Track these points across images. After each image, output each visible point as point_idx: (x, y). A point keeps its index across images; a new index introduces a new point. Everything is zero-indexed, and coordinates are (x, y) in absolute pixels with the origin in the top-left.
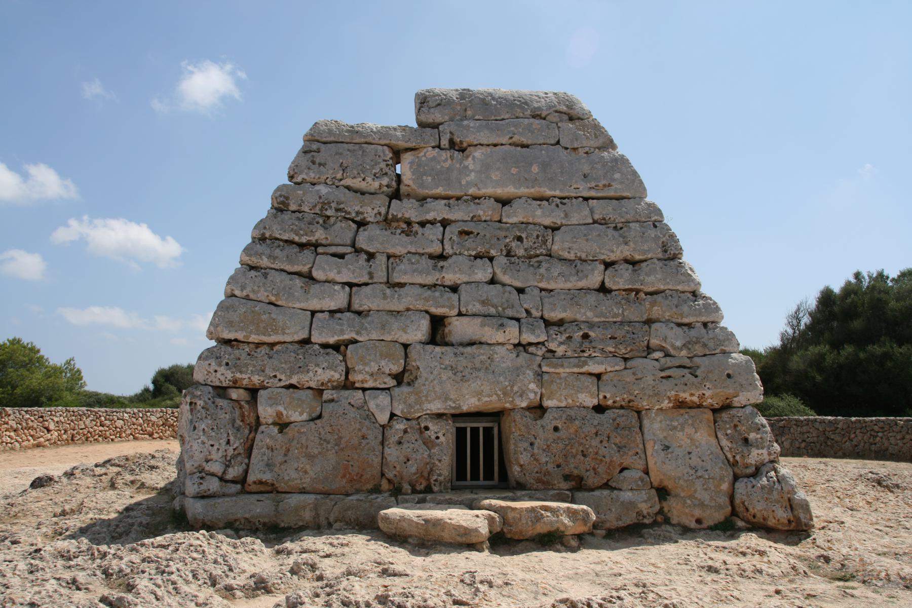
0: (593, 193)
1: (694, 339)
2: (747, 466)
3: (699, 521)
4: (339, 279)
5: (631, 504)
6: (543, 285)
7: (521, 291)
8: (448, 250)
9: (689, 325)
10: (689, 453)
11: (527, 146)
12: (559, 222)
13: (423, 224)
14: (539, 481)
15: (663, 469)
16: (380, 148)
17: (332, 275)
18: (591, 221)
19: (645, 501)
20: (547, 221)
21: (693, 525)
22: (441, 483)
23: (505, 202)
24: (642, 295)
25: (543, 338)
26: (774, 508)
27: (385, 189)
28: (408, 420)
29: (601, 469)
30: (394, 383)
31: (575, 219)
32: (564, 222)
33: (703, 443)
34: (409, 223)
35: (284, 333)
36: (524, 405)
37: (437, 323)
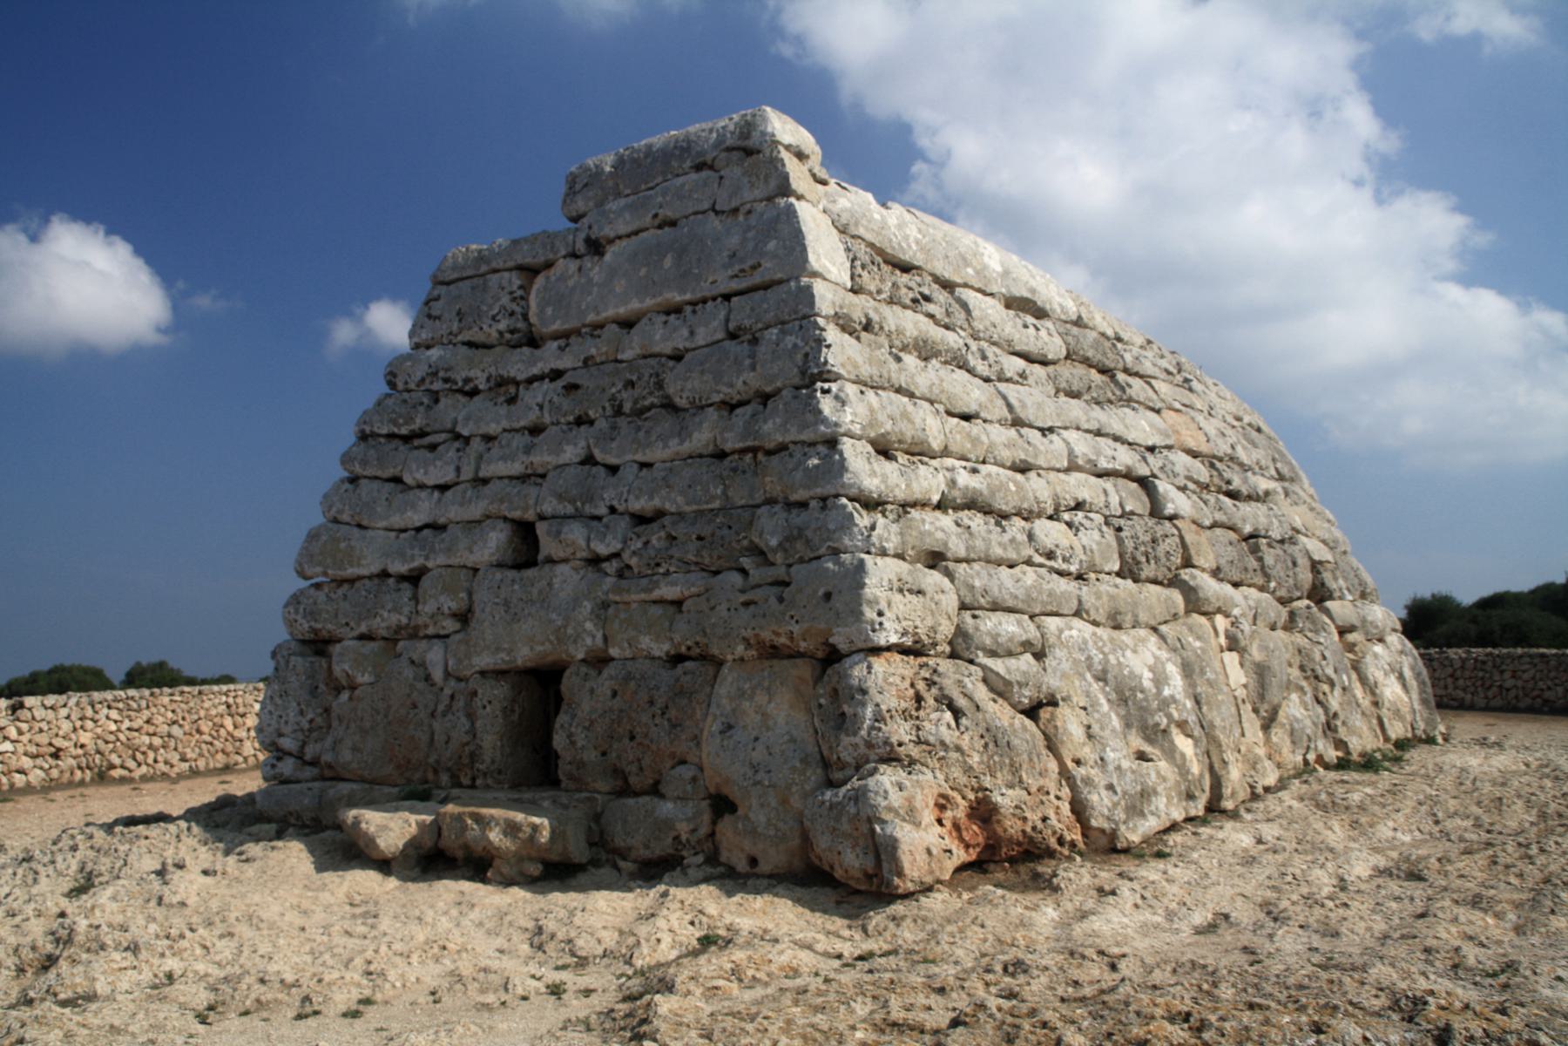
0: (735, 285)
1: (795, 533)
2: (842, 766)
3: (753, 861)
4: (431, 482)
5: (668, 824)
6: (640, 457)
7: (613, 470)
8: (547, 419)
9: (803, 505)
10: (756, 739)
11: (673, 223)
12: (681, 346)
13: (530, 381)
14: (571, 777)
15: (721, 762)
16: (506, 275)
17: (420, 476)
18: (720, 335)
19: (688, 820)
20: (667, 348)
21: (742, 866)
22: (485, 774)
23: (627, 324)
24: (760, 456)
25: (616, 546)
26: (840, 848)
27: (508, 336)
28: (459, 679)
29: (646, 762)
30: (457, 626)
31: (700, 340)
32: (688, 345)
33: (781, 720)
34: (517, 384)
35: (359, 565)
36: (580, 656)
37: (525, 532)
